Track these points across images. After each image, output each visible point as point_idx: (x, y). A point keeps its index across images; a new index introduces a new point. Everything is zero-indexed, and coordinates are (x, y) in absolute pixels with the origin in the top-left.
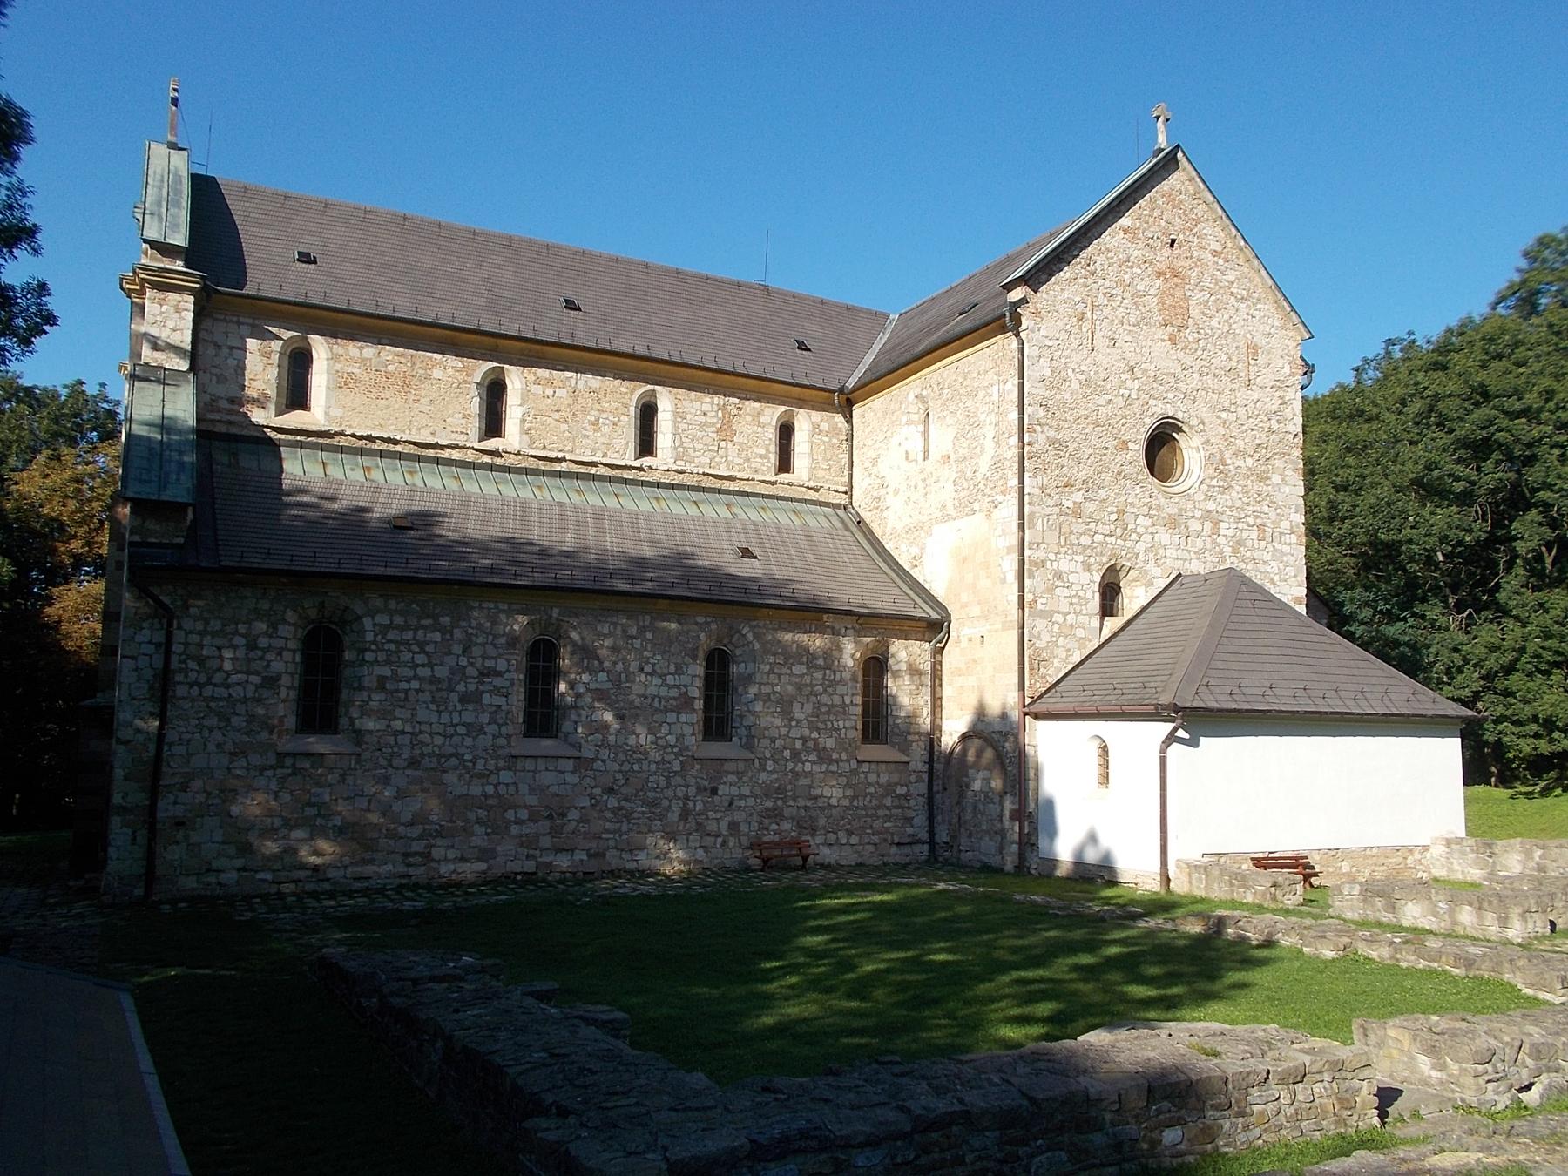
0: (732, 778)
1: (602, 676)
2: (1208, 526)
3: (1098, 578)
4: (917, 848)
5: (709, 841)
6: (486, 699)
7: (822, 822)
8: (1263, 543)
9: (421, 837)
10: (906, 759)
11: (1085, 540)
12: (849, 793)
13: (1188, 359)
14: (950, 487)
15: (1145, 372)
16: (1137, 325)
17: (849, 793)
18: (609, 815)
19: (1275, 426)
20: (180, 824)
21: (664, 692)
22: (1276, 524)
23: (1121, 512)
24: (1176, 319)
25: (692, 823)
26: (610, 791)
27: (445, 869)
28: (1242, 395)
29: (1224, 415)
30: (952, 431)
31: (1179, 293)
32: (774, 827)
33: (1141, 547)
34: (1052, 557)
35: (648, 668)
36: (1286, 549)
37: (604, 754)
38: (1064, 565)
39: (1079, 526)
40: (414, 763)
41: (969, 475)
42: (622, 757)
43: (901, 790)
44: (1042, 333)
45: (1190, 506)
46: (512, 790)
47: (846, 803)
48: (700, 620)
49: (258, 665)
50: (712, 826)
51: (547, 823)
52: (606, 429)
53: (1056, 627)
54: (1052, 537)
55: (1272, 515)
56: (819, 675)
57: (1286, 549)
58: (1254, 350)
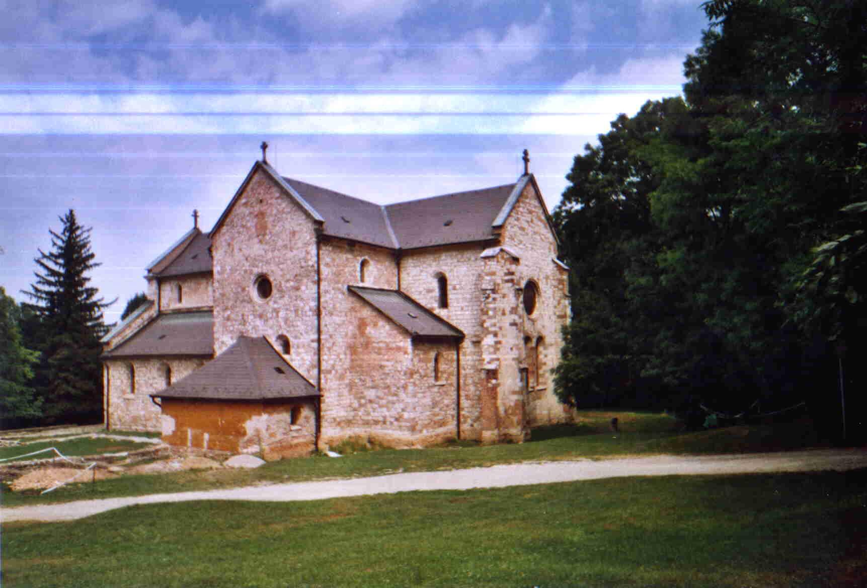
2: (274, 314)
11: (231, 328)
19: (303, 264)
22: (303, 308)
23: (243, 315)
28: (290, 255)
29: (281, 266)
39: (229, 323)
54: (221, 329)
57: (307, 318)
58: (294, 233)
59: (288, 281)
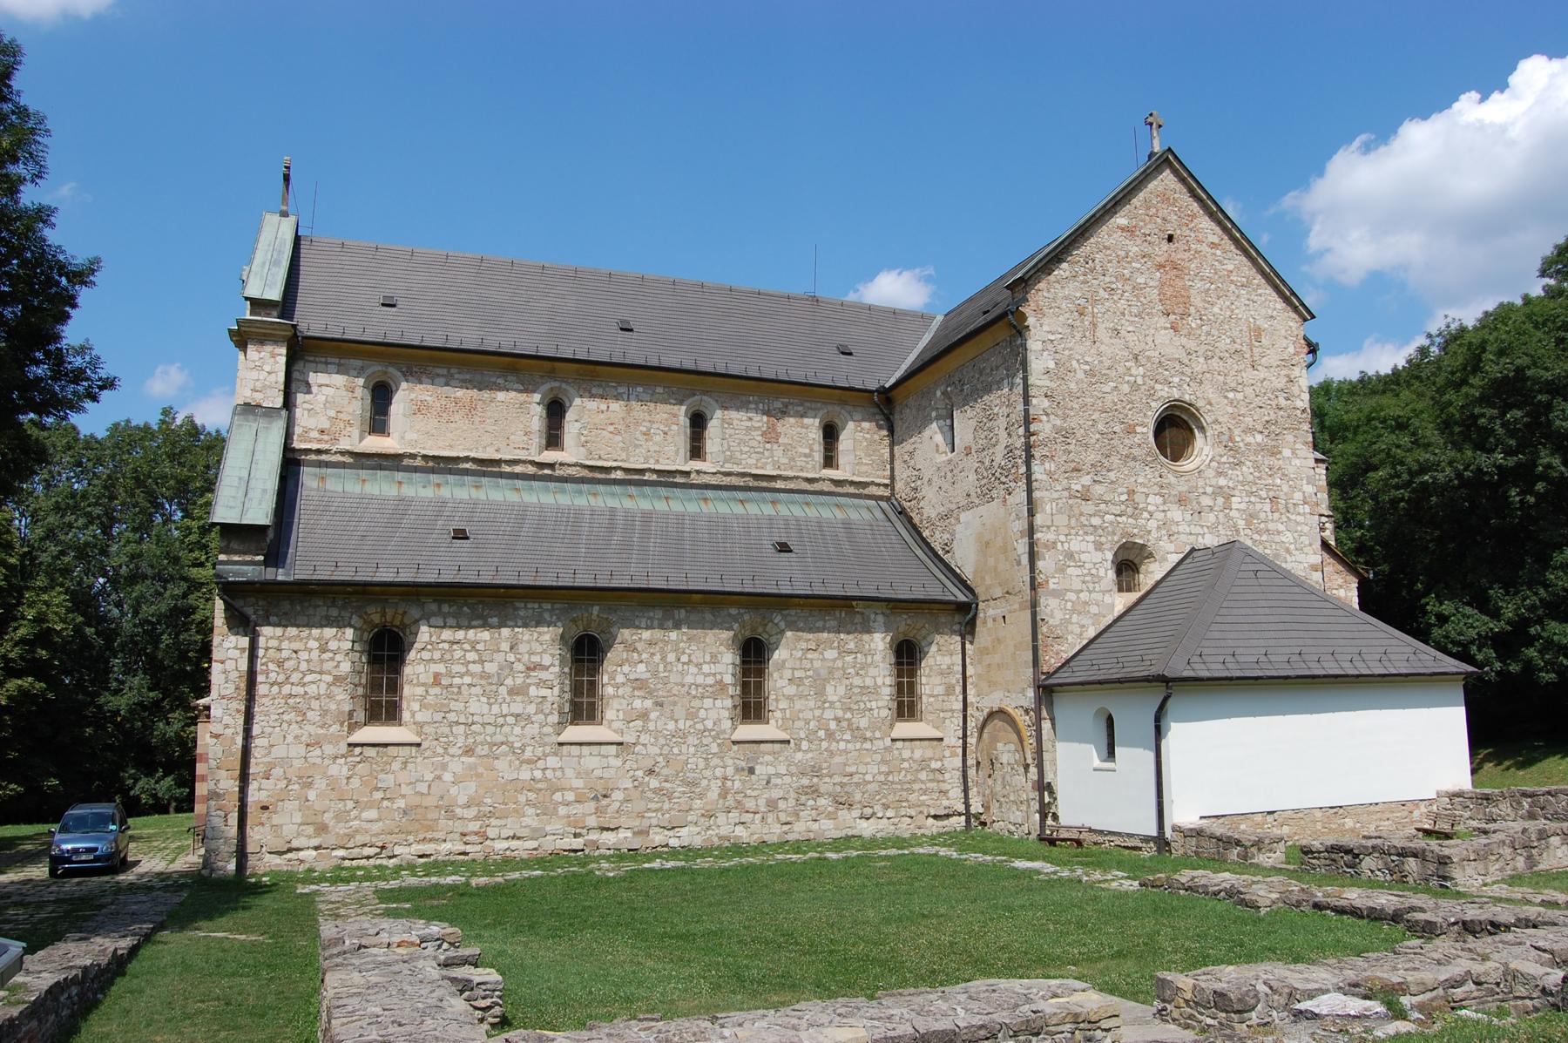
0: (768, 758)
1: (641, 667)
2: (1220, 500)
3: (1110, 556)
4: (954, 820)
5: (747, 817)
6: (533, 691)
7: (858, 797)
8: (1276, 515)
9: (476, 818)
10: (938, 734)
11: (1096, 521)
12: (884, 768)
13: (1192, 345)
14: (972, 477)
15: (1149, 358)
16: (1139, 315)
17: (884, 768)
18: (650, 795)
19: (1283, 402)
20: (265, 808)
21: (700, 679)
22: (1289, 497)
23: (1131, 492)
24: (1176, 309)
25: (730, 802)
26: (651, 772)
27: (500, 845)
28: (1249, 375)
29: (1231, 395)
30: (973, 423)
31: (1179, 283)
32: (811, 802)
33: (1152, 524)
34: (1062, 538)
35: (684, 658)
36: (1299, 519)
37: (644, 738)
38: (1075, 545)
39: (1088, 508)
40: (469, 751)
41: (987, 464)
42: (662, 741)
43: (935, 765)
44: (1046, 328)
45: (1201, 483)
46: (559, 774)
47: (882, 778)
48: (733, 611)
49: (329, 666)
50: (750, 804)
51: (593, 804)
52: (657, 438)
53: (1069, 605)
54: (1061, 520)
55: (1285, 488)
56: (849, 659)
57: (1299, 519)
58: (1258, 333)
59: (1249, 430)
